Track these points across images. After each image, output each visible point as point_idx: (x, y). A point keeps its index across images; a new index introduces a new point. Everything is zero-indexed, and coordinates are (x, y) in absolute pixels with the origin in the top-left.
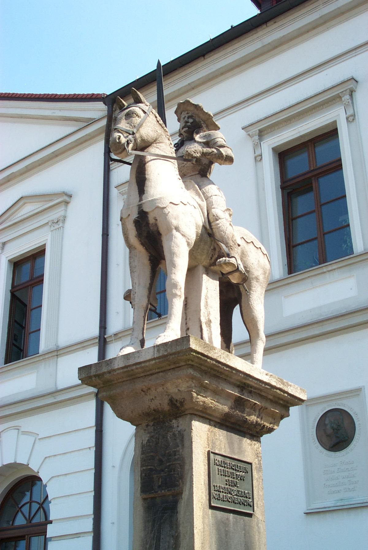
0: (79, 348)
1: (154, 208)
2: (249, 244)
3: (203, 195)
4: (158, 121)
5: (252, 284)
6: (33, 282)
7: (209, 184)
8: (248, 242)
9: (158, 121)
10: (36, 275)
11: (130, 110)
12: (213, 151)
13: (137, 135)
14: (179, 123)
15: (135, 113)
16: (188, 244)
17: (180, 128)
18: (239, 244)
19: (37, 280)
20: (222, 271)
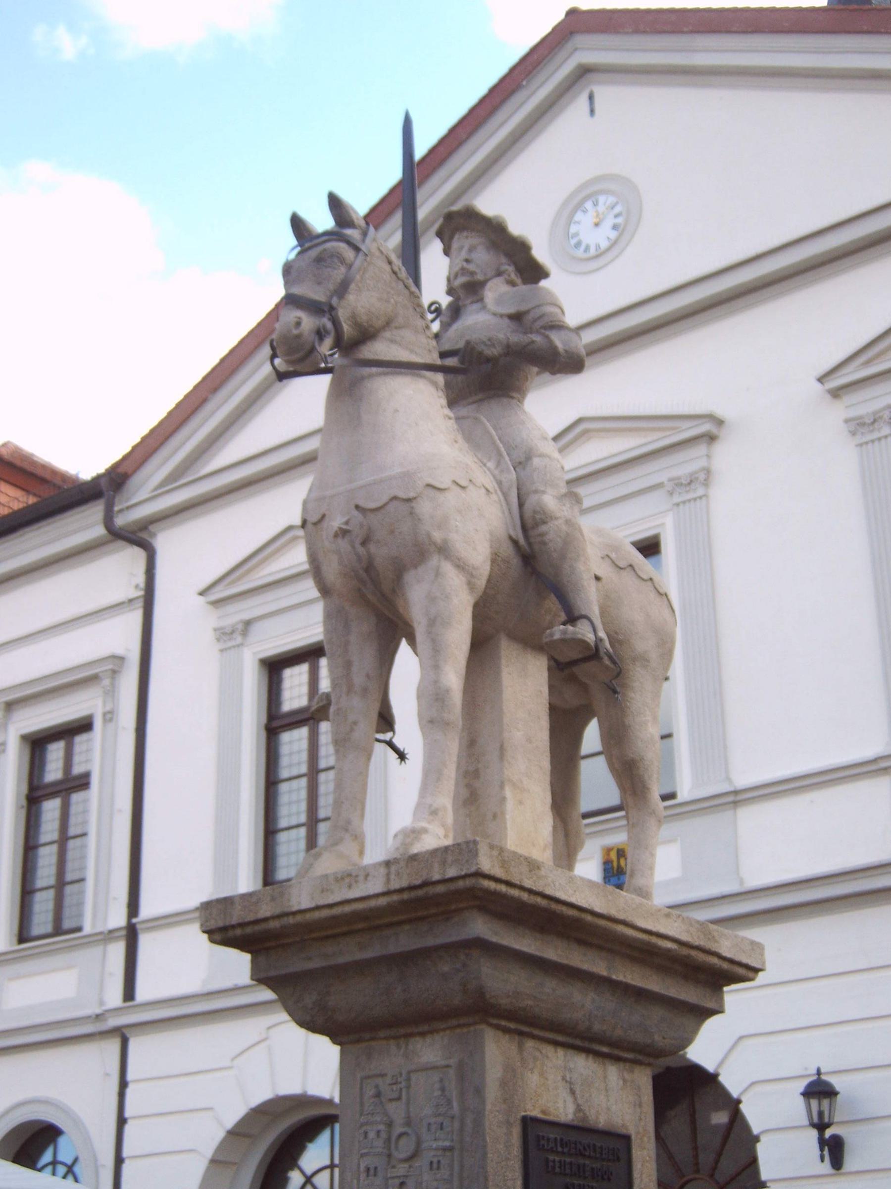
0: (190, 919)
1: (385, 499)
2: (622, 571)
3: (508, 454)
4: (395, 273)
5: (631, 673)
6: (69, 785)
7: (620, 866)
8: (622, 566)
9: (395, 273)
10: (77, 770)
11: (325, 250)
12: (533, 342)
13: (342, 314)
14: (446, 260)
15: (338, 257)
16: (471, 586)
17: (450, 273)
18: (599, 574)
19: (77, 783)
20: (557, 657)
